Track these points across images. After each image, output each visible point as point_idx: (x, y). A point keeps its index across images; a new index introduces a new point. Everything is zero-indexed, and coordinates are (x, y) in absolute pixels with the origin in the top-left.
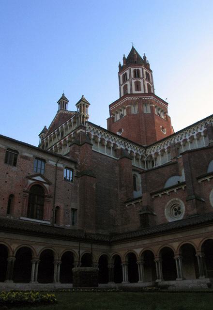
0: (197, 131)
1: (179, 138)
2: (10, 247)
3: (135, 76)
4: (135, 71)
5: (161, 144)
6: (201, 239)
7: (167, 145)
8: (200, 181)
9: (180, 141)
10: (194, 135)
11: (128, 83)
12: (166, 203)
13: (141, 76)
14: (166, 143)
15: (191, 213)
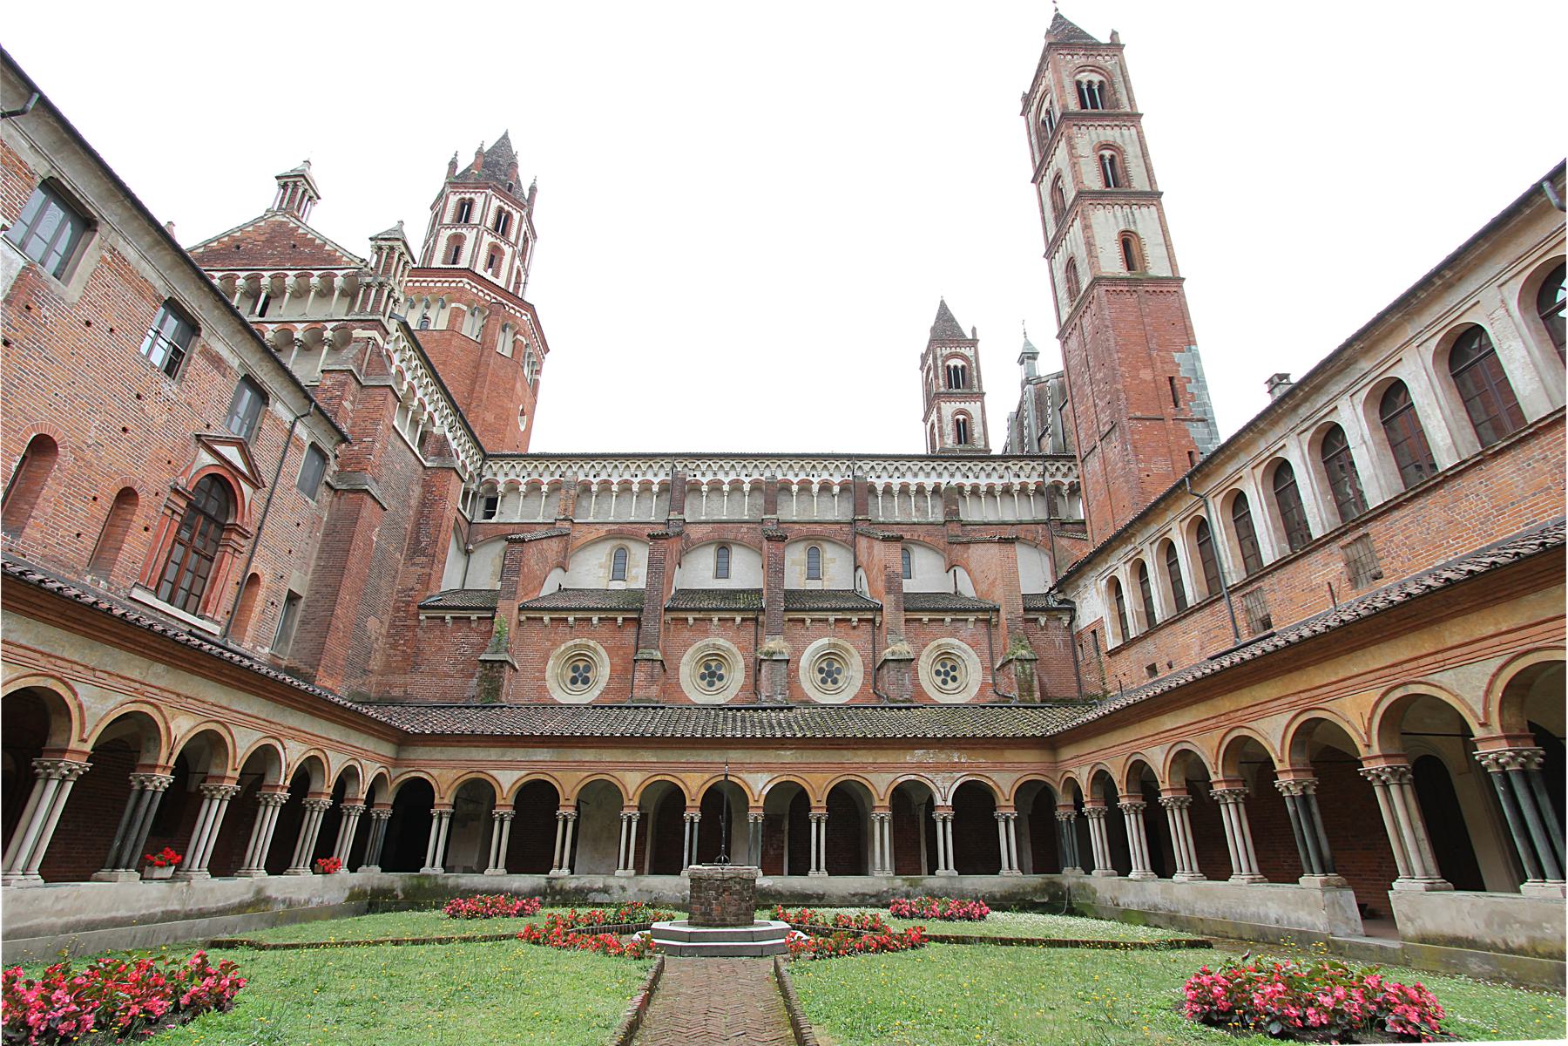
0: (644, 474)
1: (593, 473)
2: (168, 729)
3: (496, 229)
4: (500, 211)
5: (535, 463)
6: (707, 776)
7: (552, 474)
8: (668, 617)
9: (591, 478)
10: (634, 479)
11: (470, 235)
12: (555, 645)
13: (512, 238)
14: (552, 468)
15: (639, 693)
